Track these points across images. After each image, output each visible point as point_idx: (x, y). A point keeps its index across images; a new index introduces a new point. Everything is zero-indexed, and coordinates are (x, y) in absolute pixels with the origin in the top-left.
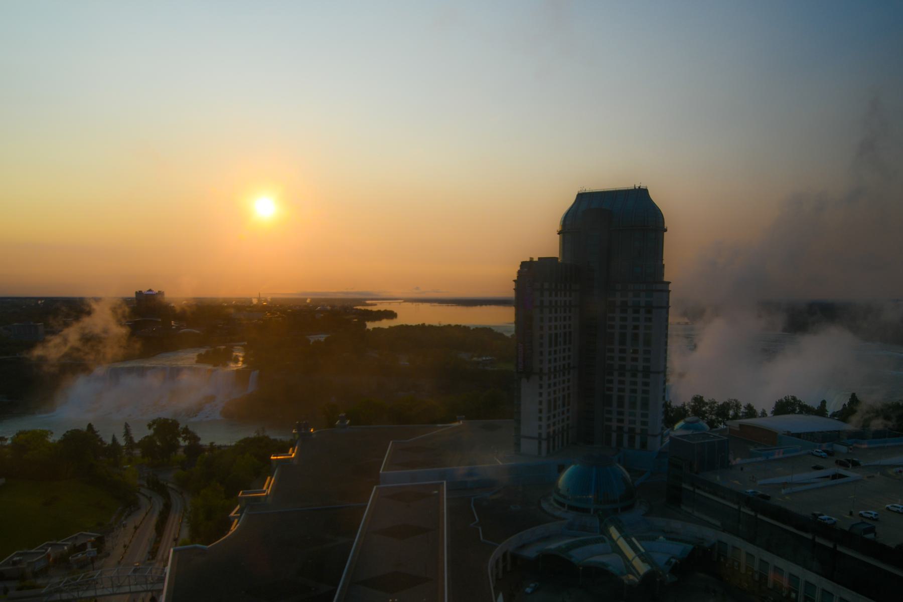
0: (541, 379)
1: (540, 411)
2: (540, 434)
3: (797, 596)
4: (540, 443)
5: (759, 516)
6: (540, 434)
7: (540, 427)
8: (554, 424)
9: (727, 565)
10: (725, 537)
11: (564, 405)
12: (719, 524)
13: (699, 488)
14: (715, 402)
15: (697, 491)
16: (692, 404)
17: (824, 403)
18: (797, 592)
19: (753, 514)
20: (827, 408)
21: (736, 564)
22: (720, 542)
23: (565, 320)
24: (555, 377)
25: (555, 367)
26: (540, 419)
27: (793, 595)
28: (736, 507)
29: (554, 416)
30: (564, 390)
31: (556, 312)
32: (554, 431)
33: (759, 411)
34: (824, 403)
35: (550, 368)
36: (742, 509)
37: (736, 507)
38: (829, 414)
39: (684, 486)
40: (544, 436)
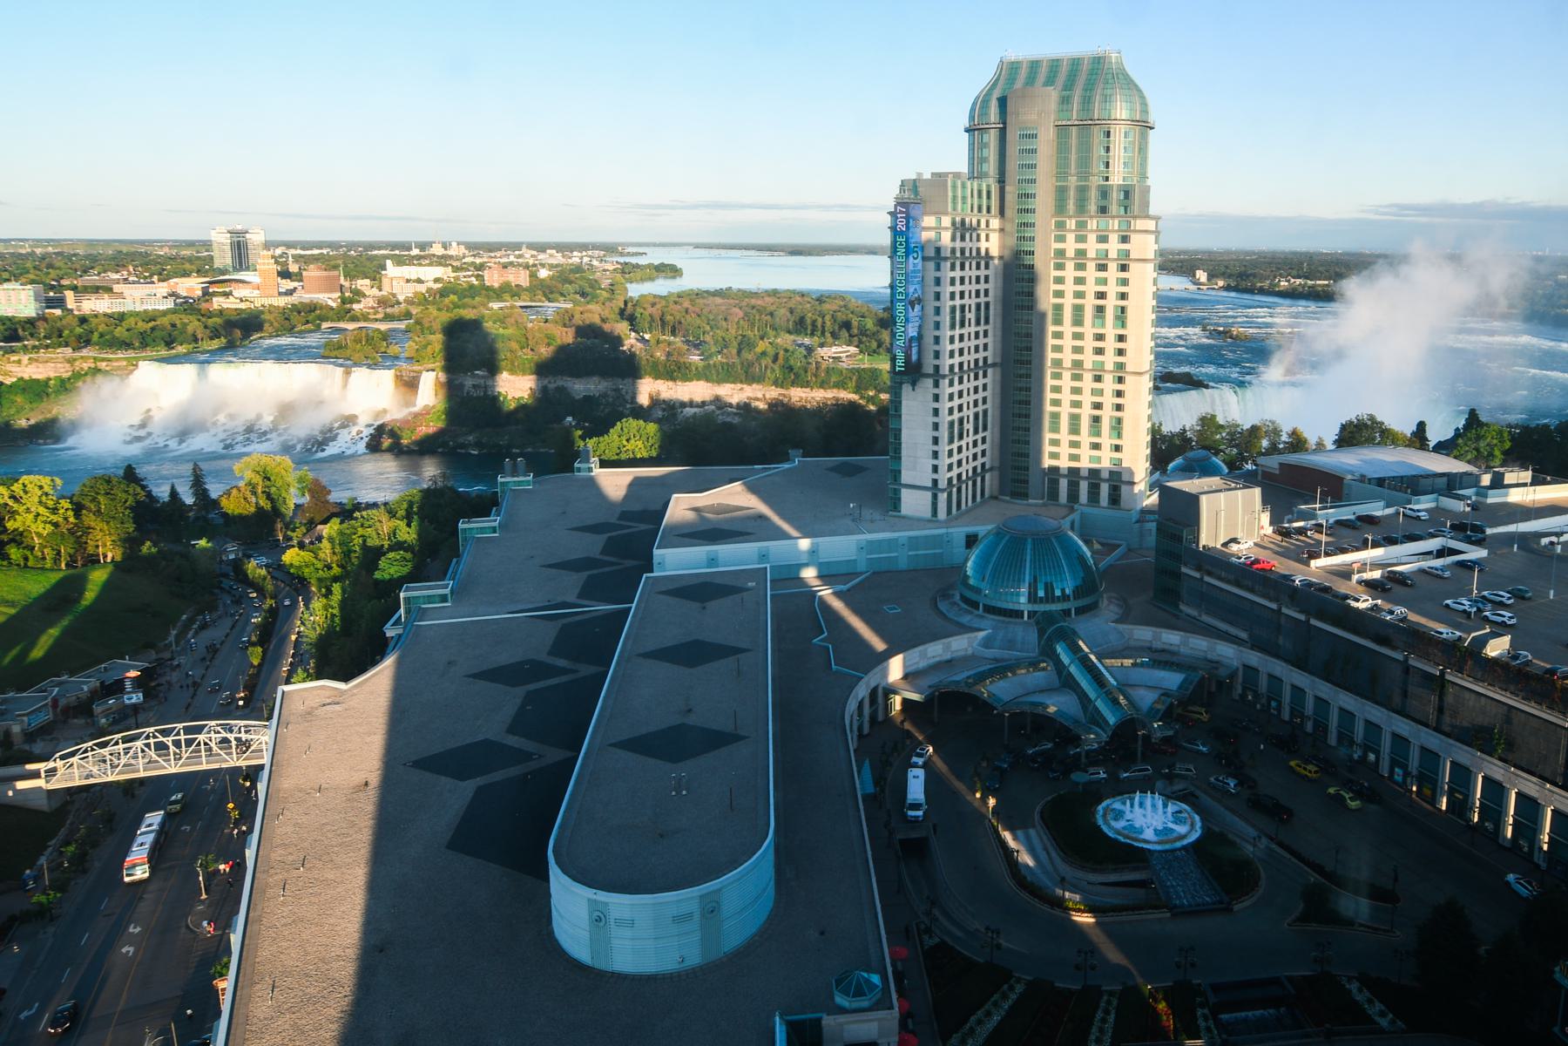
0: (936, 385)
1: (936, 441)
2: (935, 482)
3: (1377, 758)
4: (935, 497)
5: (1313, 622)
6: (935, 482)
7: (935, 469)
8: (960, 463)
9: (1258, 706)
10: (1254, 658)
11: (976, 432)
12: (1244, 635)
13: (1210, 574)
14: (1238, 426)
15: (1207, 579)
16: (1198, 428)
17: (1421, 426)
18: (1377, 753)
19: (1302, 617)
20: (1429, 435)
21: (1273, 704)
22: (1246, 666)
23: (978, 282)
24: (961, 382)
25: (961, 364)
26: (935, 455)
27: (1372, 757)
28: (1274, 606)
29: (960, 449)
30: (976, 404)
31: (963, 268)
32: (959, 476)
33: (1312, 441)
34: (1421, 426)
35: (952, 367)
36: (1285, 610)
37: (1274, 606)
38: (1432, 444)
39: (1184, 570)
40: (943, 484)
